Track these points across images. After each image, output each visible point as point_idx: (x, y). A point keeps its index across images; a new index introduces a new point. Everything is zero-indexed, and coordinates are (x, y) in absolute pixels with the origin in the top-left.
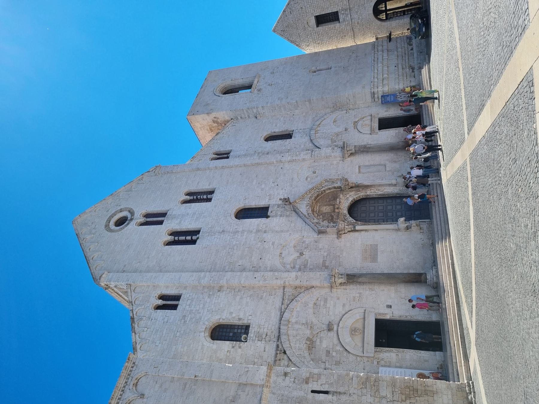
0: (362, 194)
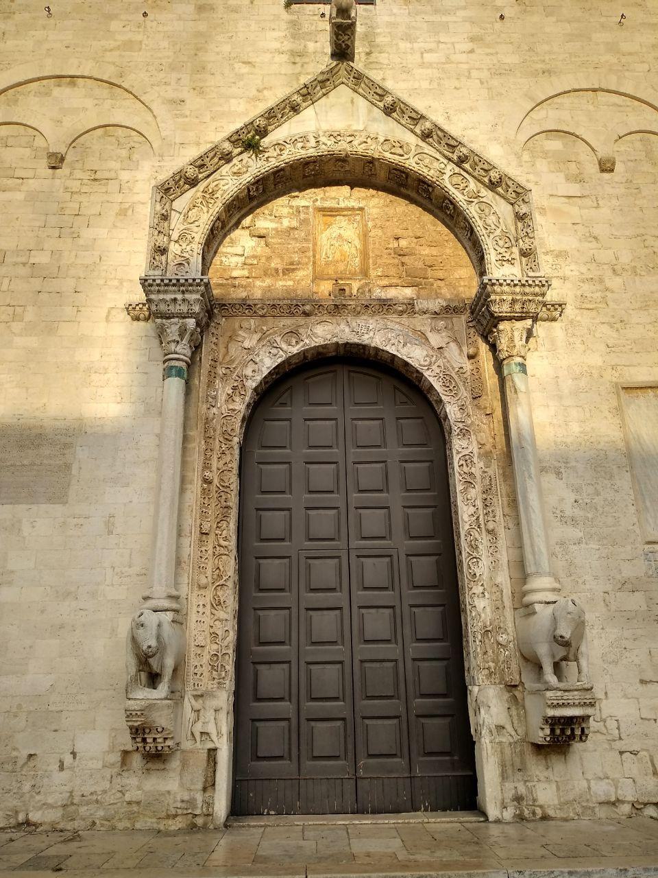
0: (452, 411)
